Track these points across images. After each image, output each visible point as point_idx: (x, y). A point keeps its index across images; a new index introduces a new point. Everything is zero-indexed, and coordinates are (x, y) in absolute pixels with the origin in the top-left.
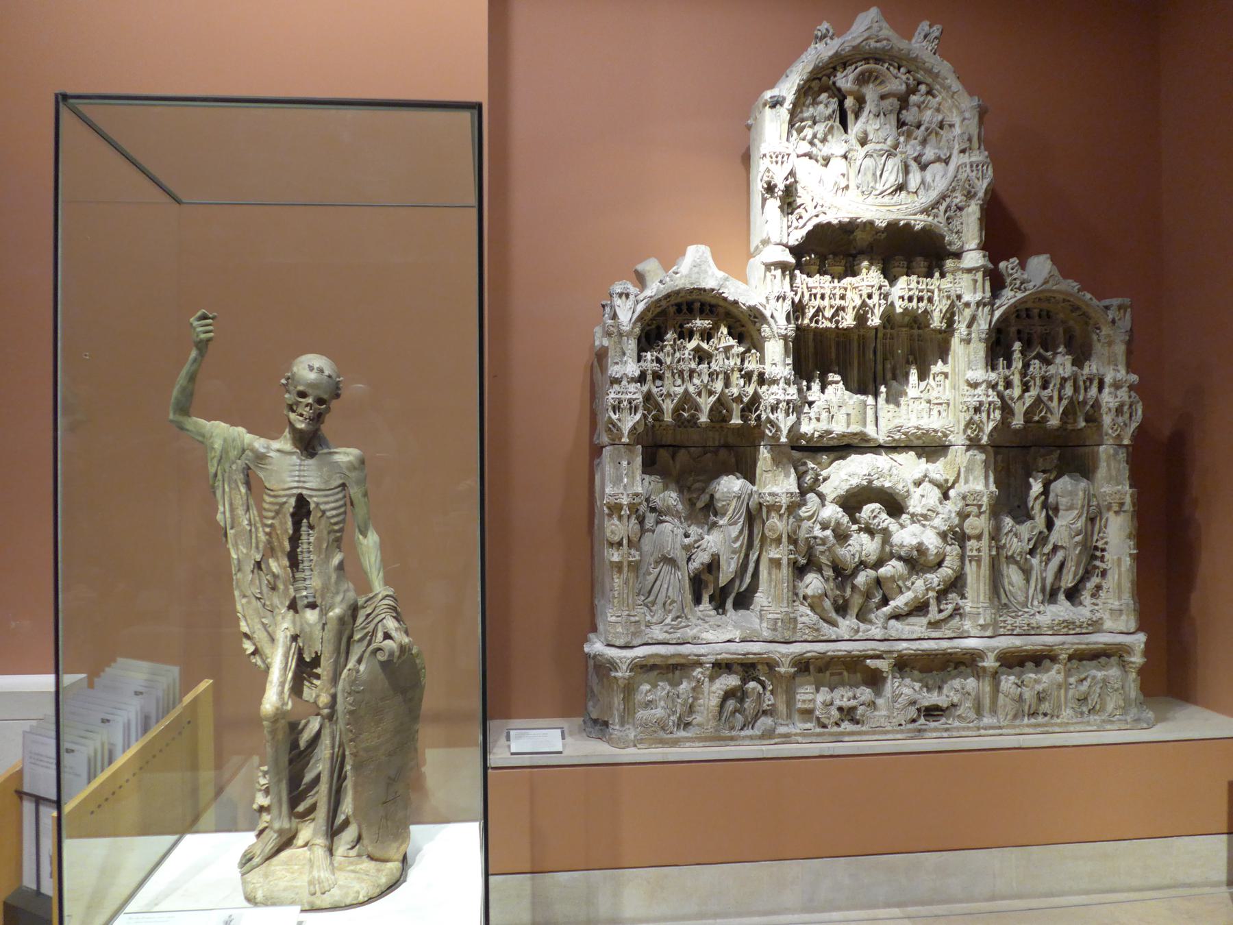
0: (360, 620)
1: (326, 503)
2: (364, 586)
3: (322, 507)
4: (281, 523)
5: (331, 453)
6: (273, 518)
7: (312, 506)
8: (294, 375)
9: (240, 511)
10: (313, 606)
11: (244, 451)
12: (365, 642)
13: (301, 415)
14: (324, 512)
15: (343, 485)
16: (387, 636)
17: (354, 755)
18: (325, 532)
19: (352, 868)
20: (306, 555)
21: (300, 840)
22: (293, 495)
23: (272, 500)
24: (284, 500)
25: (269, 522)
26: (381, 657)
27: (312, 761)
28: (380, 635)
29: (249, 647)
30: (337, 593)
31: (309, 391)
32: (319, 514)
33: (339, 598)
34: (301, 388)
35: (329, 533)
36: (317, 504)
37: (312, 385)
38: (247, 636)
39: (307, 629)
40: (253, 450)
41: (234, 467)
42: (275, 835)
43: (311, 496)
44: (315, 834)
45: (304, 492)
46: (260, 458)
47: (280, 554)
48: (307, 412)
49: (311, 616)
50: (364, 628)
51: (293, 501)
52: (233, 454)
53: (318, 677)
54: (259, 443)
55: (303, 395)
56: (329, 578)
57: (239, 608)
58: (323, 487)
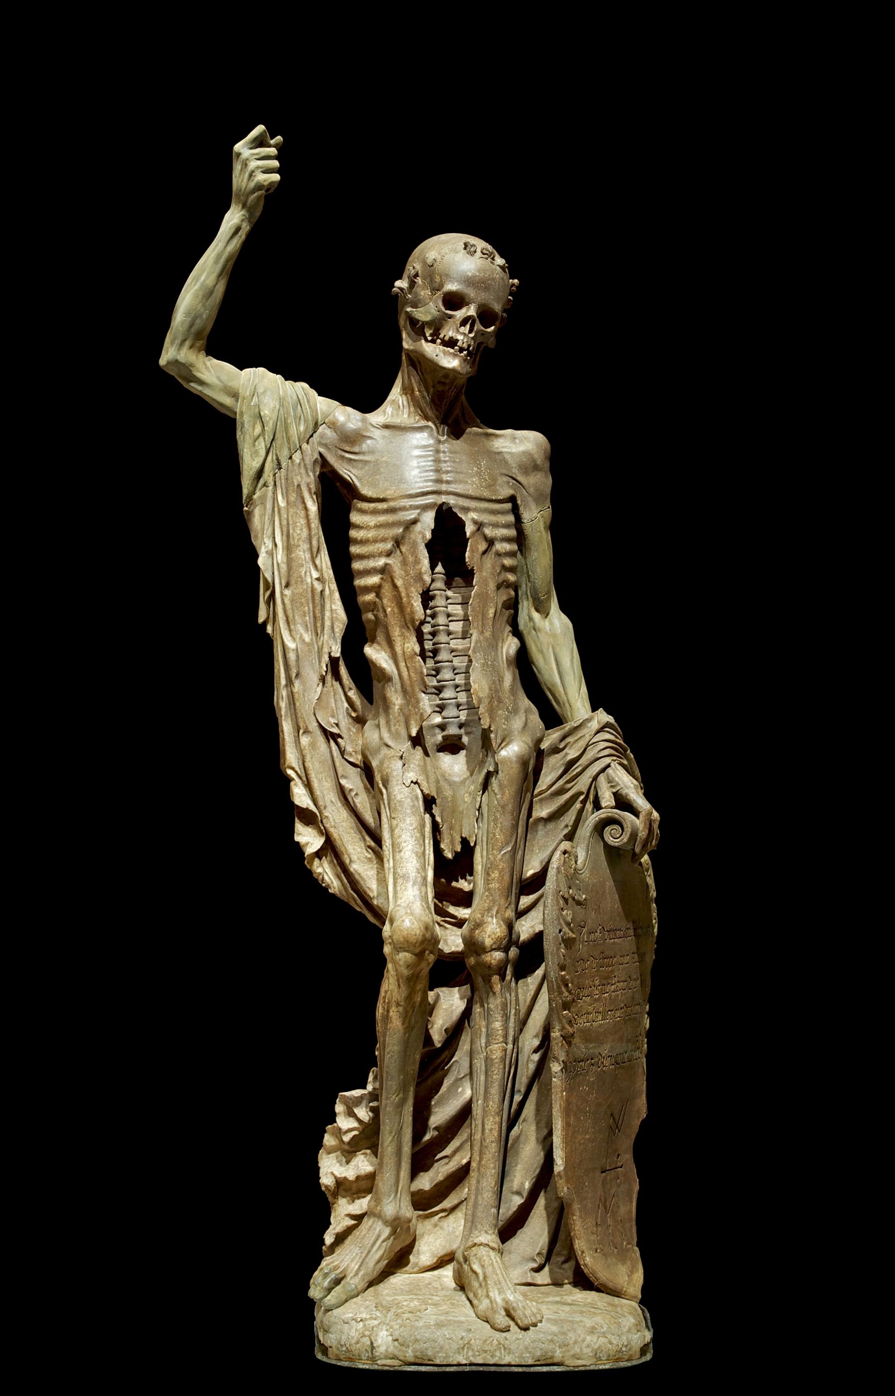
0: (547, 778)
1: (496, 525)
2: (551, 716)
3: (488, 531)
4: (404, 563)
5: (488, 435)
6: (389, 554)
7: (469, 529)
8: (430, 267)
9: (302, 554)
10: (451, 746)
11: (316, 426)
12: (570, 817)
13: (451, 343)
14: (491, 542)
15: (512, 499)
16: (623, 803)
17: (567, 1039)
18: (492, 586)
19: (558, 1299)
20: (442, 638)
21: (424, 1253)
22: (425, 508)
23: (382, 518)
24: (412, 515)
25: (381, 562)
26: (613, 836)
27: (447, 1083)
28: (607, 799)
29: (308, 839)
30: (515, 711)
31: (471, 293)
32: (483, 546)
33: (517, 723)
34: (451, 287)
35: (499, 587)
36: (479, 526)
37: (470, 281)
38: (310, 819)
39: (448, 793)
40: (333, 425)
41: (297, 457)
42: (387, 1231)
43: (466, 510)
44: (472, 1224)
45: (451, 500)
46: (350, 440)
47: (396, 632)
48: (463, 336)
49: (454, 765)
50: (561, 792)
51: (428, 519)
52: (298, 429)
53: (466, 900)
54: (347, 416)
55: (454, 301)
56: (501, 680)
57: (291, 756)
58: (486, 494)
